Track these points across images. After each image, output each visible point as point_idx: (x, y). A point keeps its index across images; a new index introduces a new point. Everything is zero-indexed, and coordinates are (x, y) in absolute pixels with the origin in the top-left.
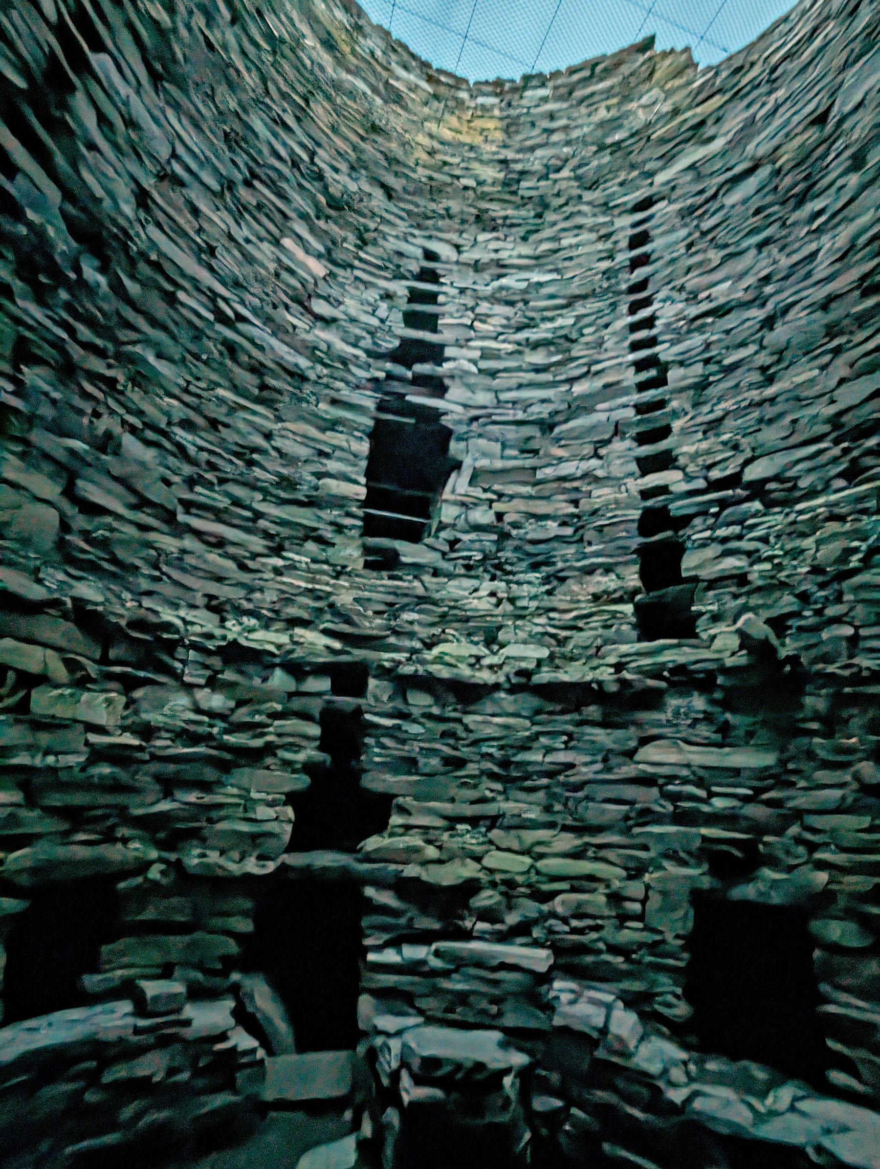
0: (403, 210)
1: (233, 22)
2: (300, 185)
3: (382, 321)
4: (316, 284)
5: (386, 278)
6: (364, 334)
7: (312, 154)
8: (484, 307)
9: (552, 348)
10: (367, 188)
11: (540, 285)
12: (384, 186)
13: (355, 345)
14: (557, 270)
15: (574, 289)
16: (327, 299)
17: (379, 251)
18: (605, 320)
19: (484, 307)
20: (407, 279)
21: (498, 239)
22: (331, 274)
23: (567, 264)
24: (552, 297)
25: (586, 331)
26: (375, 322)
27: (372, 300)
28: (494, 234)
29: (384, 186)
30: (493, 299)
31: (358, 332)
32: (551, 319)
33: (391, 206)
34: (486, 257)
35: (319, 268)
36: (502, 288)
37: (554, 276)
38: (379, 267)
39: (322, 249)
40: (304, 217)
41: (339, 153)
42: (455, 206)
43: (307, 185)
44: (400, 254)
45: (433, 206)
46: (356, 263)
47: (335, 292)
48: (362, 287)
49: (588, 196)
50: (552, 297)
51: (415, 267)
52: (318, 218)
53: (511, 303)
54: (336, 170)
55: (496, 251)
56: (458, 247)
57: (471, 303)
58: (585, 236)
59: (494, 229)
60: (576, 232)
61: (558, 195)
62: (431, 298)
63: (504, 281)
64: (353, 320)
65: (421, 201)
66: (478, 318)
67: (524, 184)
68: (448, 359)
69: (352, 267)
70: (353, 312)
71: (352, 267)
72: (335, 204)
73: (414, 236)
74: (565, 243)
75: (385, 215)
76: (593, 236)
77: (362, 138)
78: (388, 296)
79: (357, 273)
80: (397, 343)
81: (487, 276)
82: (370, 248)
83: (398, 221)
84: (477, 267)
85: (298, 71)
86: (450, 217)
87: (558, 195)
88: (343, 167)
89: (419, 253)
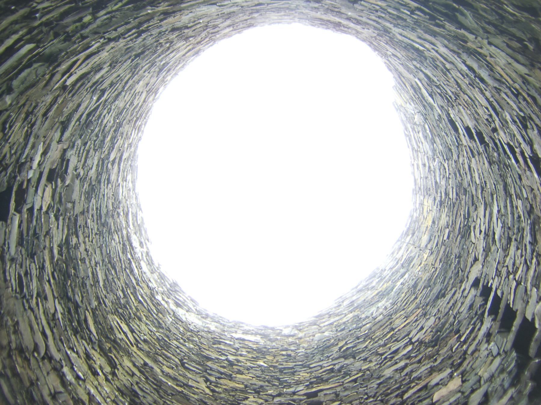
0: (451, 289)
1: (354, 358)
2: (419, 362)
3: (499, 354)
4: (463, 393)
5: (479, 329)
6: (502, 377)
7: (411, 342)
8: (509, 261)
9: (537, 227)
10: (435, 311)
11: (499, 211)
12: (437, 298)
13: (505, 392)
14: (492, 195)
15: (501, 187)
16: (473, 391)
17: (465, 322)
18: (516, 176)
19: (509, 261)
20: (484, 311)
21: (475, 227)
22: (463, 374)
23: (488, 185)
24: (505, 207)
25: (525, 196)
26: (498, 361)
27: (486, 353)
28: (472, 228)
29: (437, 298)
30: (506, 250)
31: (498, 381)
32: (519, 217)
33: (448, 297)
34: (481, 245)
35: (455, 384)
36: (500, 240)
37: (495, 196)
38: (473, 329)
39: (449, 371)
40: (432, 371)
41: (416, 321)
42: (456, 251)
43: (420, 356)
44: (471, 307)
45: (453, 266)
46: (465, 347)
47: (472, 379)
48: (476, 354)
49: (455, 157)
50: (505, 207)
51: (479, 301)
52: (436, 360)
53: (509, 240)
54: (422, 328)
55: (481, 231)
56: (476, 260)
57: (504, 271)
58: (473, 165)
59: (469, 227)
60: (472, 169)
61: (455, 175)
62: (497, 300)
63: (497, 237)
64: (492, 377)
65: (450, 274)
66: (515, 272)
67: (451, 196)
68: (533, 319)
69: (465, 352)
70: (486, 375)
71: (465, 352)
72: (436, 341)
73: (464, 290)
74: (478, 182)
75: (449, 306)
76: (473, 160)
77: (416, 298)
78: (488, 336)
79: (469, 352)
80: (514, 354)
81: (493, 248)
82: (462, 330)
83: (455, 297)
84: (487, 250)
85: (381, 326)
86: (460, 257)
87: (455, 175)
88: (422, 321)
89: (473, 292)
